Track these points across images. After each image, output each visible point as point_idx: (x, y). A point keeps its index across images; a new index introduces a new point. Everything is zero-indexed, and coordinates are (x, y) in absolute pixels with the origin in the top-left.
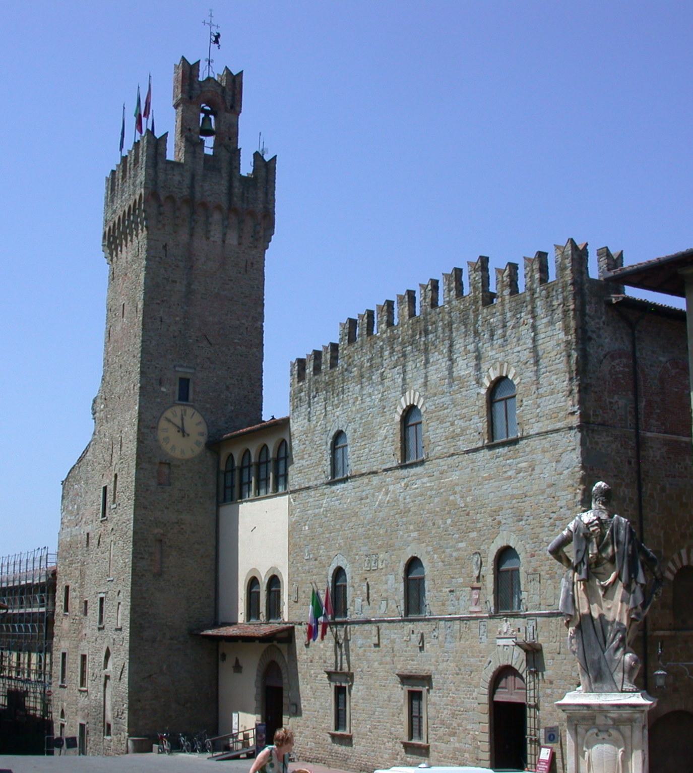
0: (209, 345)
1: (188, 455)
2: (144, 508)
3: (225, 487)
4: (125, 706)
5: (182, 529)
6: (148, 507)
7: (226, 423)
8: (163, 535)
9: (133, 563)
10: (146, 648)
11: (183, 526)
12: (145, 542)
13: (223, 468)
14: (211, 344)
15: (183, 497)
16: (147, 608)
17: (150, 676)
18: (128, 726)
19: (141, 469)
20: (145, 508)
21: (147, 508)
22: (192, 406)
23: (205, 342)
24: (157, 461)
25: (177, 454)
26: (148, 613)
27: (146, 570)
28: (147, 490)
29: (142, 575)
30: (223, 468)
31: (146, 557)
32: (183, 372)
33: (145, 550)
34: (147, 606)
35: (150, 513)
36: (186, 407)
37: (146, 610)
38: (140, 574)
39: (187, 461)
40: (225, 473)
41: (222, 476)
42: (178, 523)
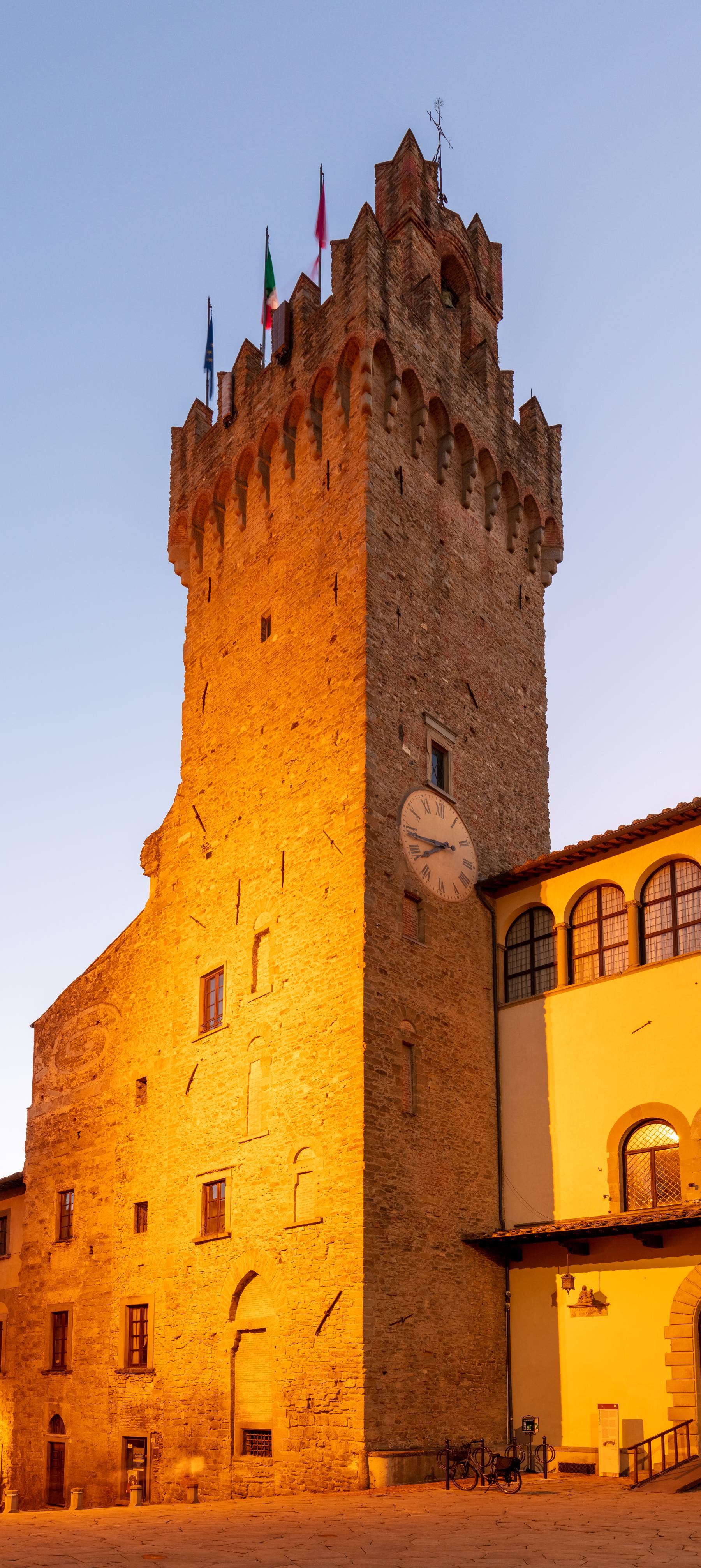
0: (473, 706)
1: (449, 895)
2: (381, 971)
3: (507, 978)
4: (350, 1383)
5: (446, 1034)
6: (389, 972)
7: (501, 861)
8: (413, 1035)
9: (366, 1079)
10: (393, 1260)
11: (446, 1029)
12: (385, 1042)
13: (501, 941)
14: (475, 704)
15: (445, 974)
16: (393, 1178)
17: (402, 1320)
18: (366, 1427)
19: (374, 889)
20: (383, 972)
21: (386, 973)
22: (452, 803)
23: (468, 697)
24: (401, 885)
25: (432, 886)
26: (395, 1188)
27: (390, 1099)
28: (386, 938)
29: (384, 1109)
30: (501, 941)
31: (389, 1072)
32: (438, 733)
33: (385, 1058)
34: (394, 1174)
35: (392, 986)
36: (446, 804)
37: (391, 1182)
38: (380, 1105)
39: (450, 904)
40: (509, 948)
41: (501, 955)
42: (438, 1019)
